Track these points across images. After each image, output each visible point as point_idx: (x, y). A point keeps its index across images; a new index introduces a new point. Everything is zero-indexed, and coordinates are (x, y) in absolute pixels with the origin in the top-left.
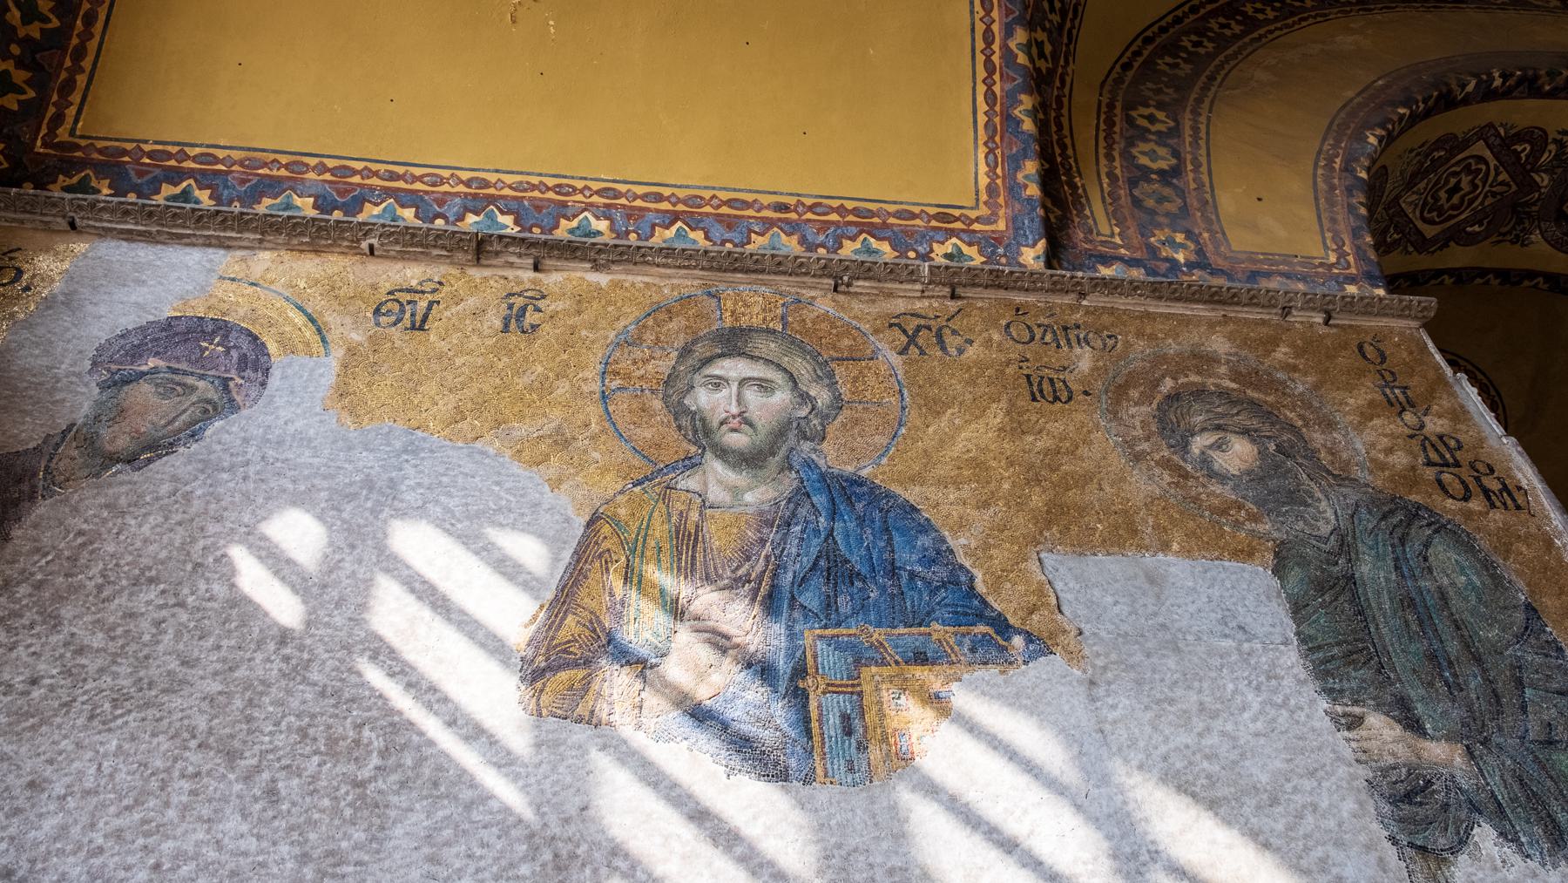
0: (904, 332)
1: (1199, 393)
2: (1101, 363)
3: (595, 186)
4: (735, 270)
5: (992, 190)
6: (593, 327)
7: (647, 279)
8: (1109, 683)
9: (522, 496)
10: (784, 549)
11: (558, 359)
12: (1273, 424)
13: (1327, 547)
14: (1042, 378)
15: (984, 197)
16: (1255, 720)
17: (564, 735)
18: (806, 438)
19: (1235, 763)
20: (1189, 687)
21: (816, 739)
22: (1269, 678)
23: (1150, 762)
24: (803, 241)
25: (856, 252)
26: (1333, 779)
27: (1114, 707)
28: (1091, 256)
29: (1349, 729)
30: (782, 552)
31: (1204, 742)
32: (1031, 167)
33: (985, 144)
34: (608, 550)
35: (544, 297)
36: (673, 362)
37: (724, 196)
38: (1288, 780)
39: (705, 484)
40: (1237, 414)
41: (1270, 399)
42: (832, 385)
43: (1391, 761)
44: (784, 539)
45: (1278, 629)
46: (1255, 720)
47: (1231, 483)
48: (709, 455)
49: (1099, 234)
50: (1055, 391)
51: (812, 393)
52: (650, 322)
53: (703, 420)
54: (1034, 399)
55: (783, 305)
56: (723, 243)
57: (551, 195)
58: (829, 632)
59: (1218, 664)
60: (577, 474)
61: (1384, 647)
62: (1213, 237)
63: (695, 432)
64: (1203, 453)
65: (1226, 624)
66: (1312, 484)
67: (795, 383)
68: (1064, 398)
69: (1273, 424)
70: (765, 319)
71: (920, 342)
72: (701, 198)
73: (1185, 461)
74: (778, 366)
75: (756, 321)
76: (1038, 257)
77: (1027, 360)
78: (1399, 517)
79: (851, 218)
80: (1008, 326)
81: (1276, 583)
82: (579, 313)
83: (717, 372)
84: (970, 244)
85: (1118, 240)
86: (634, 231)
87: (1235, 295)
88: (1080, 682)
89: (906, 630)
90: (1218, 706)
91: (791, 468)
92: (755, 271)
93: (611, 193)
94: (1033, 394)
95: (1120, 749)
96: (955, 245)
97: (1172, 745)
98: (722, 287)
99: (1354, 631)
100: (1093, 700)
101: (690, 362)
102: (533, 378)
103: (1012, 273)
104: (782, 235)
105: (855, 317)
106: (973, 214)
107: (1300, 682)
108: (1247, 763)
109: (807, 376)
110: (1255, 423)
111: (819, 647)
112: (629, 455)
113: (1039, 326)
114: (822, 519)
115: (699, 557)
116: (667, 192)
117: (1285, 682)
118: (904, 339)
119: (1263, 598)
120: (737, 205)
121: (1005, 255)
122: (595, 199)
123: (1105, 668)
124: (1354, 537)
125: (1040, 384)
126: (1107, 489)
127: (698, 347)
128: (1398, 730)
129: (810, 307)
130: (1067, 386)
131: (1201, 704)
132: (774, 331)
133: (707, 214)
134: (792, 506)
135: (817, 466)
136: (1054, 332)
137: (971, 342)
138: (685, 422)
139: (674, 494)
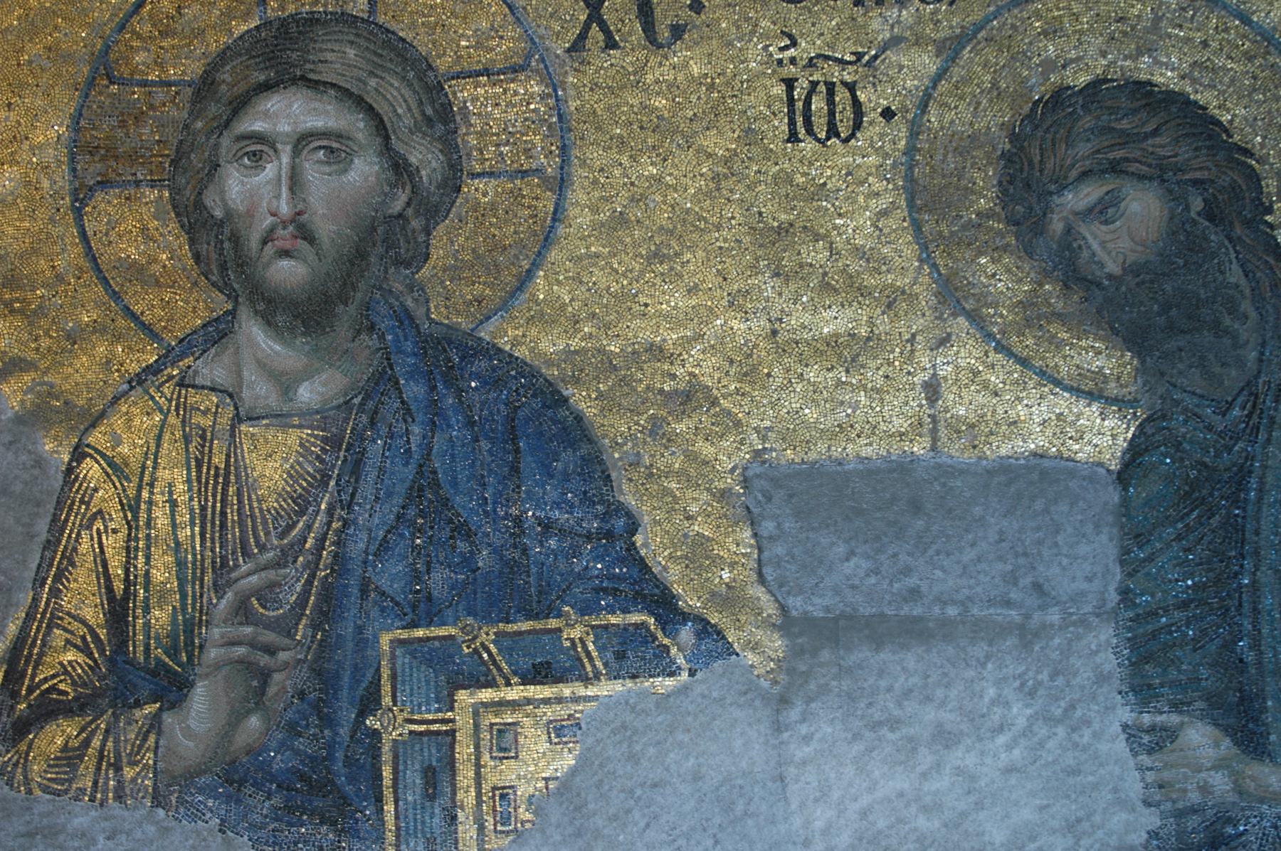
8: (809, 700)
10: (355, 490)
14: (814, 84)
16: (1009, 748)
17: (62, 819)
18: (400, 262)
19: (963, 815)
20: (928, 699)
21: (389, 808)
22: (1052, 677)
23: (842, 821)
26: (1100, 834)
27: (807, 739)
29: (1150, 752)
30: (353, 495)
31: (926, 787)
34: (100, 512)
38: (1033, 839)
40: (1155, 133)
43: (1194, 797)
44: (356, 467)
45: (1097, 584)
46: (1009, 748)
48: (244, 313)
50: (832, 113)
51: (413, 160)
53: (235, 239)
58: (420, 633)
59: (981, 655)
61: (1256, 611)
63: (223, 267)
64: (1068, 230)
65: (1015, 584)
66: (1243, 282)
73: (1029, 252)
74: (361, 103)
77: (794, 44)
81: (1114, 496)
83: (258, 126)
88: (766, 698)
89: (525, 626)
90: (964, 727)
91: (372, 328)
94: (792, 123)
95: (802, 805)
97: (879, 794)
99: (1218, 580)
100: (778, 728)
101: (213, 109)
107: (1101, 679)
108: (982, 815)
109: (408, 121)
110: (1184, 152)
111: (399, 662)
112: (121, 322)
114: (416, 429)
115: (232, 516)
117: (1078, 680)
119: (1089, 529)
123: (807, 675)
127: (225, 75)
128: (1226, 743)
130: (856, 103)
131: (940, 725)
134: (370, 404)
139: (194, 398)
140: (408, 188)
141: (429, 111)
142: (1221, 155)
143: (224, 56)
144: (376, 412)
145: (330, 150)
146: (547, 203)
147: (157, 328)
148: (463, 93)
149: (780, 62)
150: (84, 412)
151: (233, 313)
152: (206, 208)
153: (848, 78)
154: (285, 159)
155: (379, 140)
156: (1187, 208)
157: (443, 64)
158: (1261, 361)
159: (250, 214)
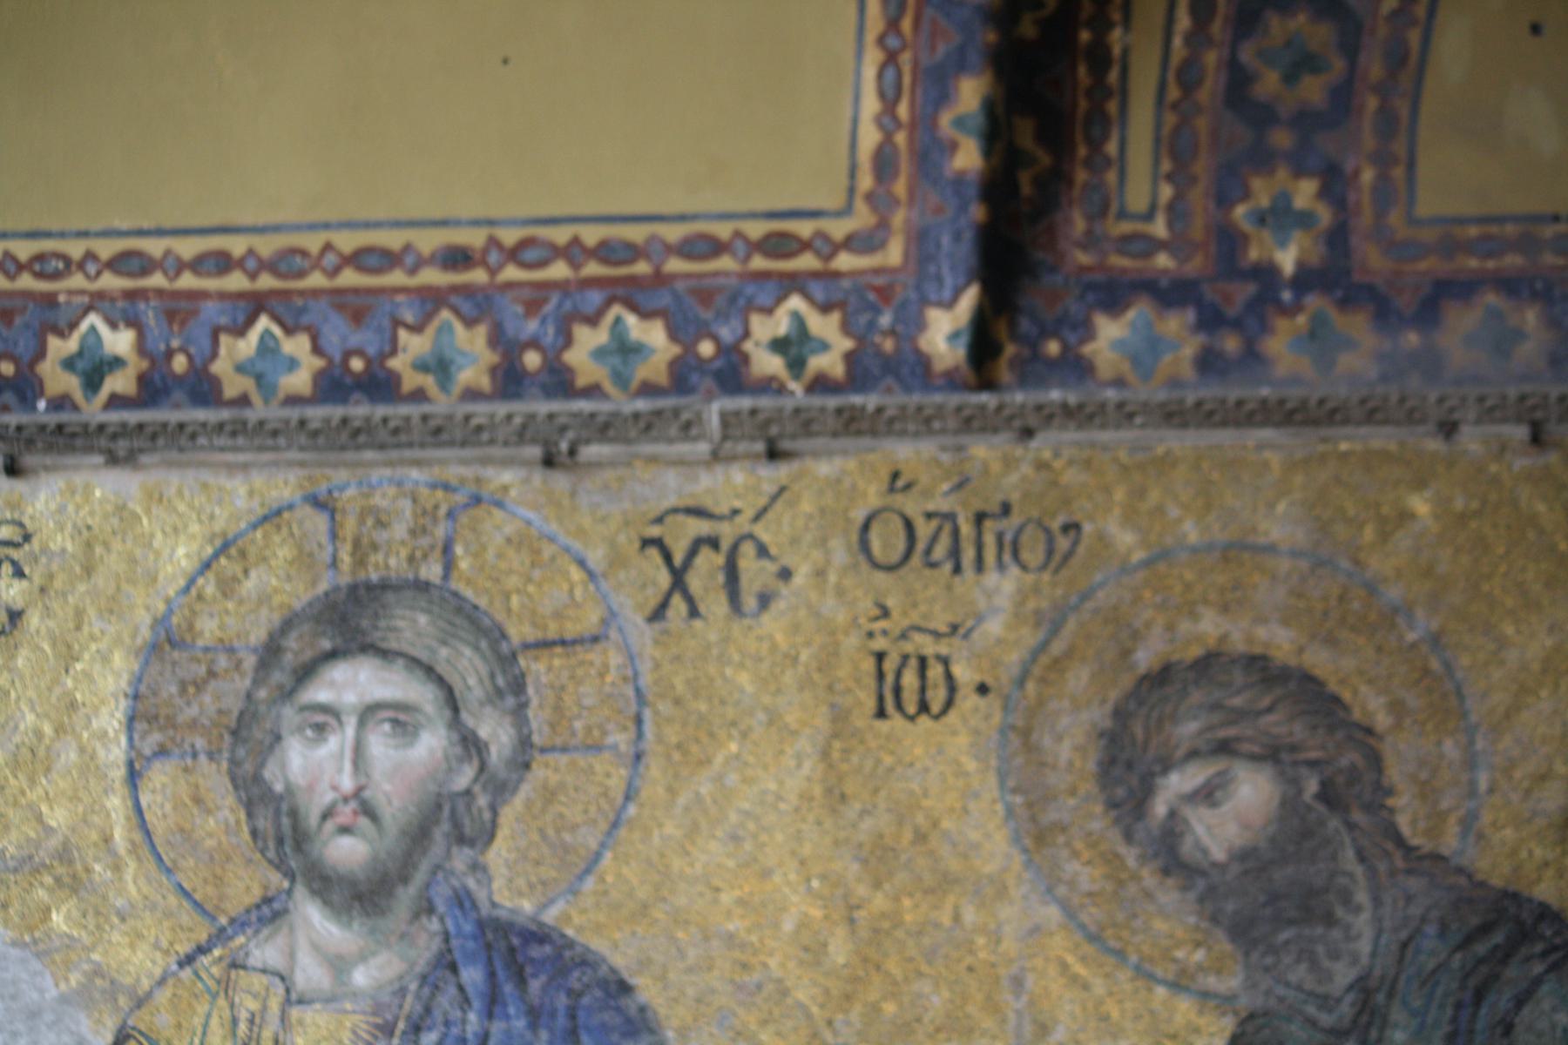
0: (667, 557)
1: (1208, 665)
2: (1031, 604)
3: (107, 249)
4: (358, 448)
5: (884, 163)
6: (113, 607)
7: (207, 476)
9: (13, 997)
11: (57, 691)
12: (1331, 729)
13: (1326, 1019)
15: (866, 182)
18: (461, 839)
24: (496, 339)
25: (599, 354)
28: (1090, 287)
32: (970, 93)
33: (881, 41)
35: (27, 538)
36: (248, 682)
37: (347, 242)
39: (292, 956)
40: (1270, 710)
41: (1348, 663)
42: (519, 713)
47: (1201, 884)
49: (1123, 215)
50: (923, 689)
51: (484, 732)
52: (208, 586)
53: (294, 814)
54: (881, 713)
55: (450, 515)
56: (348, 355)
57: (26, 282)
60: (89, 949)
62: (1383, 178)
63: (280, 841)
64: (1173, 814)
66: (1359, 870)
67: (455, 709)
68: (937, 698)
69: (1331, 729)
70: (411, 559)
71: (694, 582)
72: (304, 253)
73: (1128, 837)
74: (430, 672)
75: (396, 564)
76: (953, 337)
77: (885, 613)
78: (1498, 938)
79: (593, 269)
80: (866, 527)
82: (89, 570)
84: (825, 308)
85: (1159, 228)
86: (183, 350)
87: (1334, 411)
91: (430, 910)
92: (398, 446)
93: (135, 264)
94: (881, 699)
96: (797, 318)
98: (341, 475)
101: (278, 677)
102: (17, 739)
103: (880, 410)
104: (459, 328)
105: (581, 533)
106: (838, 229)
109: (478, 692)
110: (1299, 731)
112: (173, 900)
113: (929, 516)
116: (237, 246)
118: (664, 579)
120: (373, 261)
121: (892, 332)
122: (111, 282)
124: (1391, 995)
125: (899, 674)
126: (970, 915)
127: (291, 642)
129: (498, 514)
130: (949, 676)
132: (423, 587)
133: (315, 293)
134: (426, 991)
135: (475, 906)
136: (956, 533)
137: (785, 574)
138: (263, 823)
140: (476, 762)
141: (501, 681)
142: (1340, 735)
143: (288, 625)
144: (433, 996)
145: (396, 722)
146: (617, 780)
147: (209, 907)
148: (537, 669)
149: (870, 635)
150: (131, 992)
151: (289, 892)
152: (264, 781)
153: (943, 650)
154: (350, 731)
155: (448, 713)
156: (1300, 792)
157: (518, 632)
158: (1374, 954)
159: (311, 788)
